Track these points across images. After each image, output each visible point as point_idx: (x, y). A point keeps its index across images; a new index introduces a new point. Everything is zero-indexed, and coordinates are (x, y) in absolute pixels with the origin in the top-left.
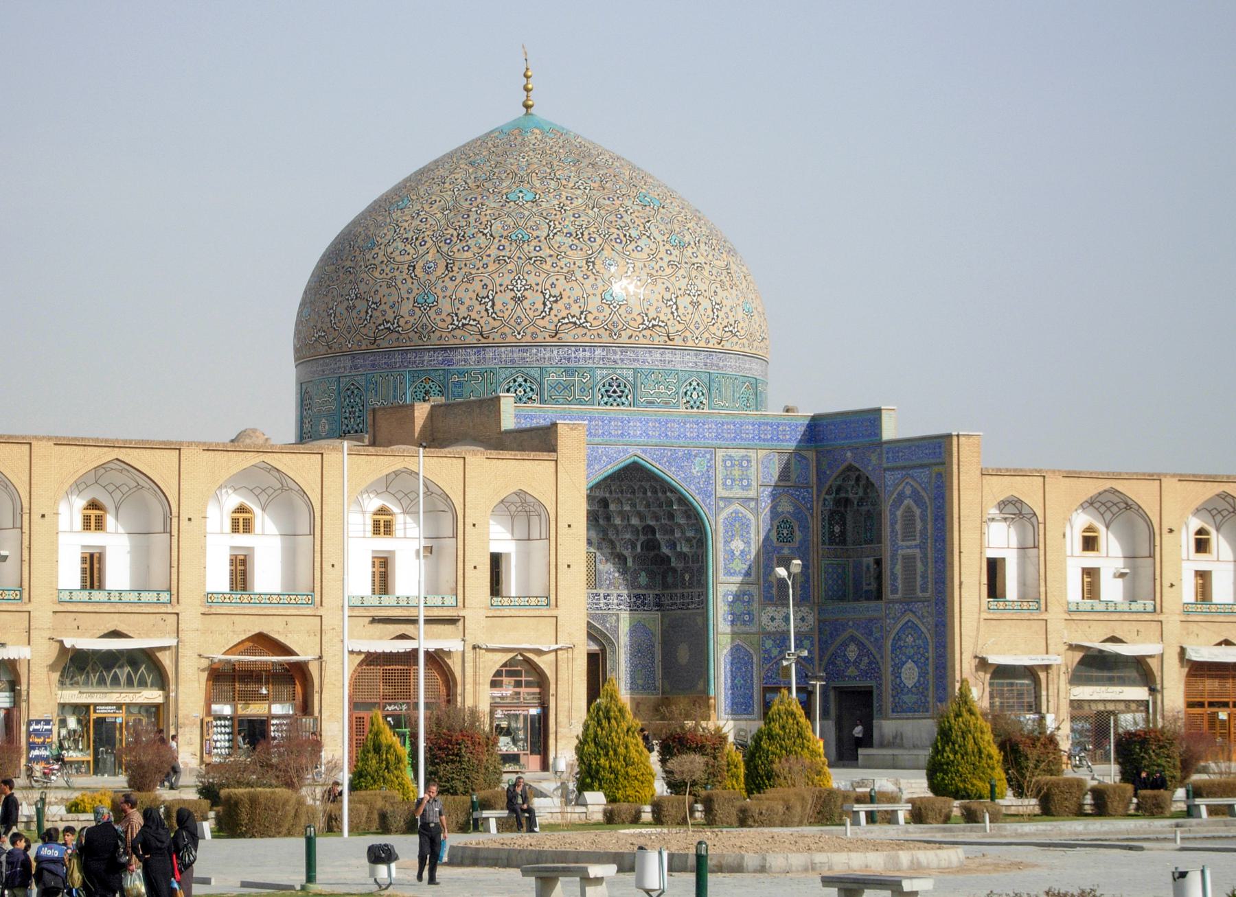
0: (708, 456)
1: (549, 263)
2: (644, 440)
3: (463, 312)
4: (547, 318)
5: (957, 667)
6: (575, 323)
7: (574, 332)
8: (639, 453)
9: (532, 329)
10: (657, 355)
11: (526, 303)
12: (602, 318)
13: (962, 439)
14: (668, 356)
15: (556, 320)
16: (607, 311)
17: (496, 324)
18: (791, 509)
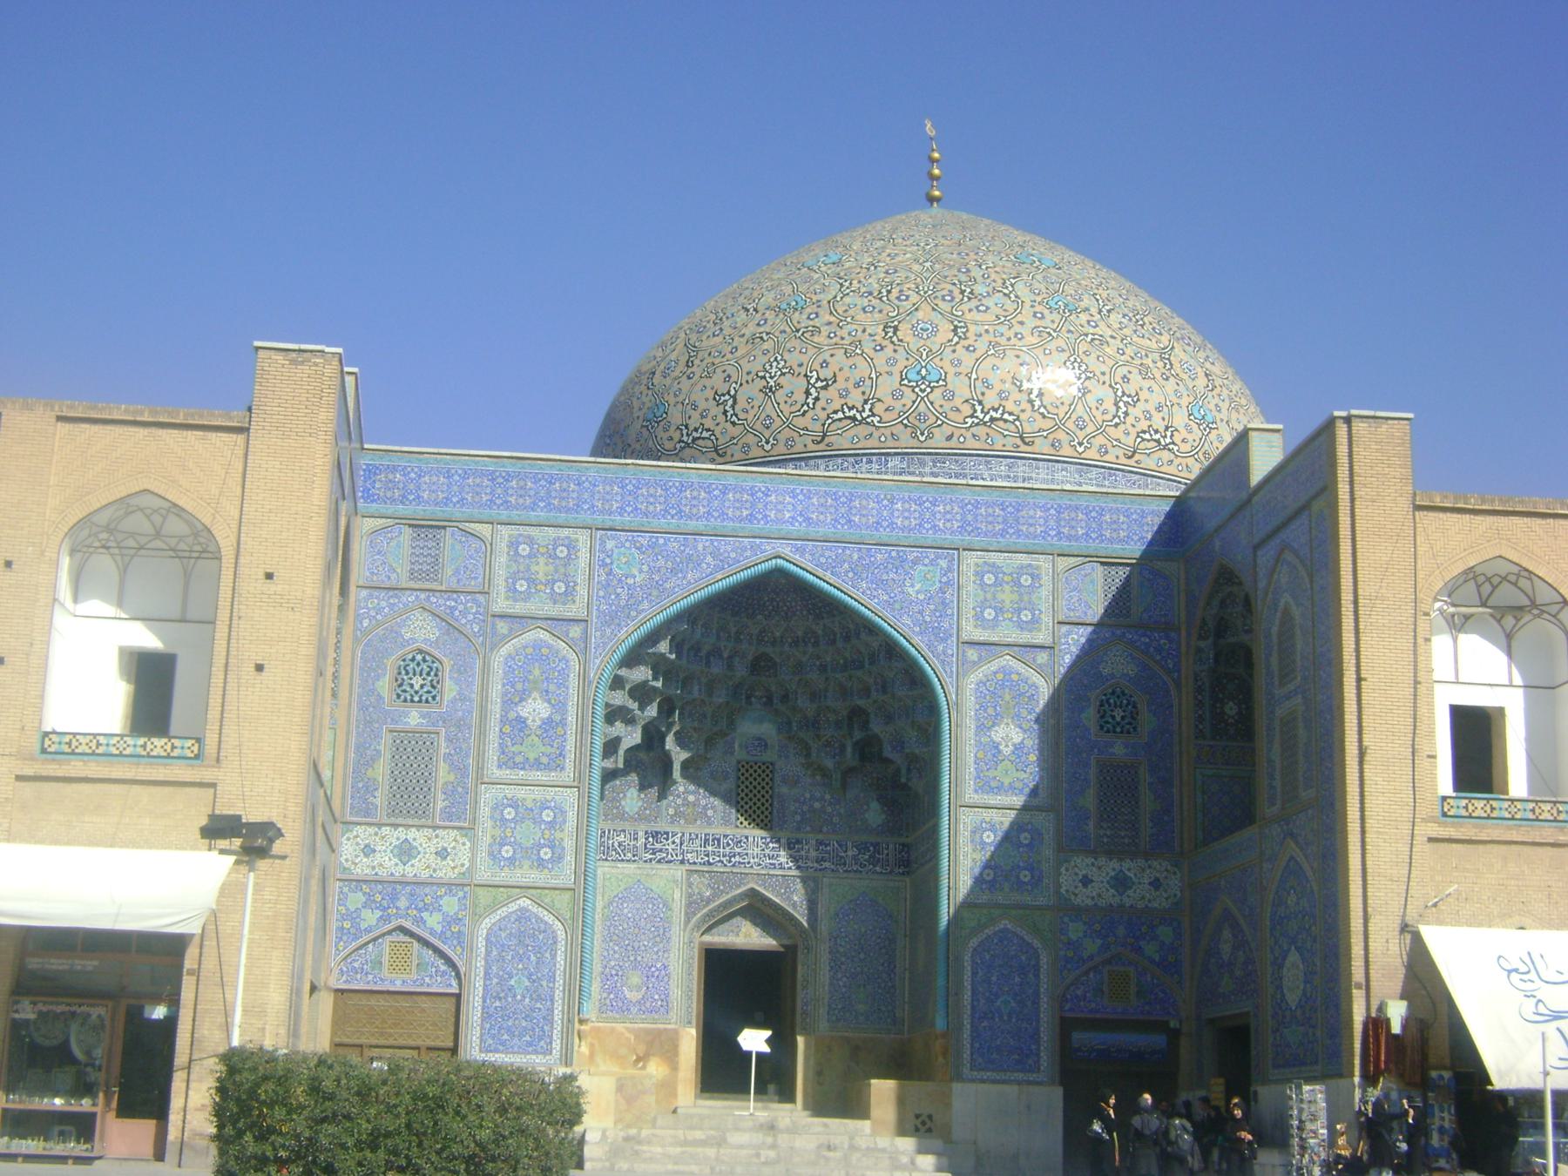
0: (943, 563)
1: (824, 333)
2: (798, 528)
3: (693, 424)
4: (811, 413)
5: (1357, 950)
6: (853, 419)
7: (852, 432)
8: (786, 551)
9: (787, 433)
10: (1002, 467)
11: (780, 395)
12: (898, 405)
13: (1358, 426)
14: (1022, 469)
15: (823, 415)
16: (909, 396)
17: (736, 431)
18: (1131, 670)
